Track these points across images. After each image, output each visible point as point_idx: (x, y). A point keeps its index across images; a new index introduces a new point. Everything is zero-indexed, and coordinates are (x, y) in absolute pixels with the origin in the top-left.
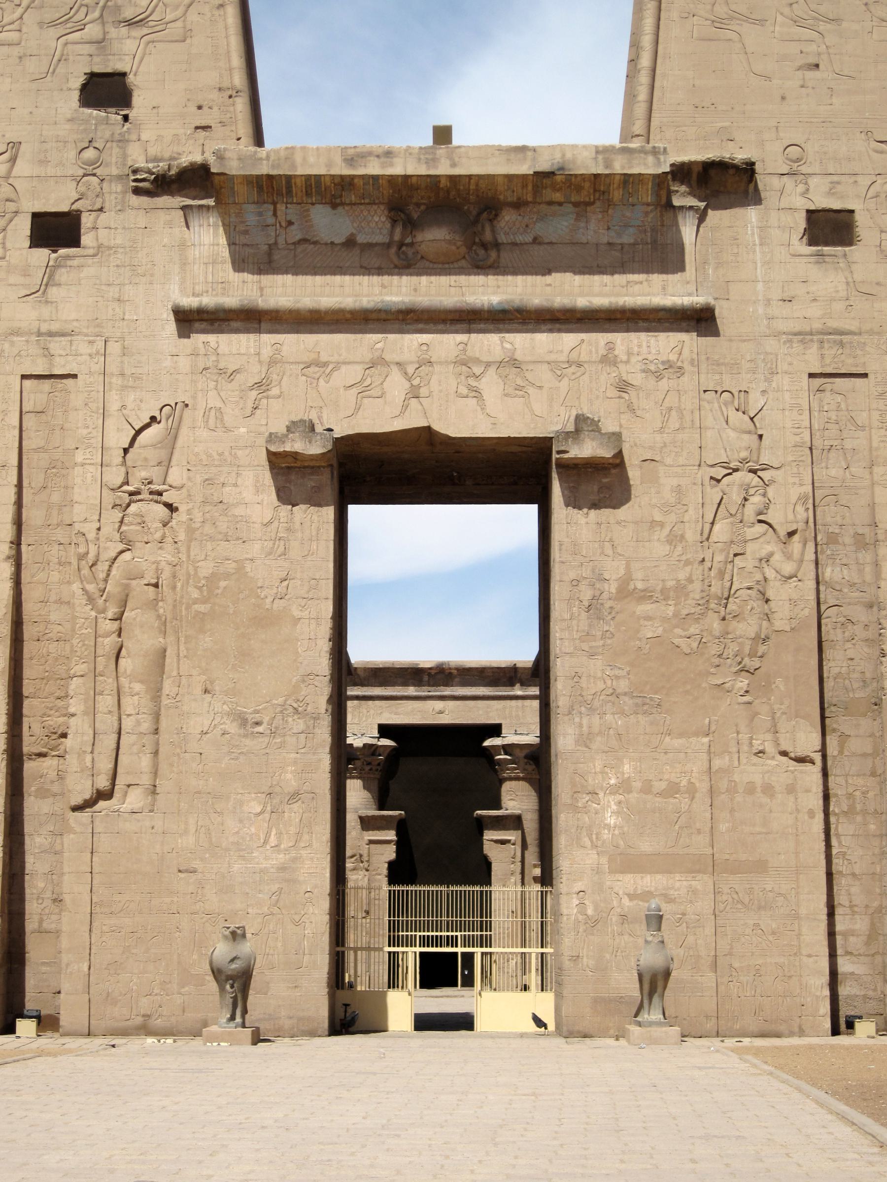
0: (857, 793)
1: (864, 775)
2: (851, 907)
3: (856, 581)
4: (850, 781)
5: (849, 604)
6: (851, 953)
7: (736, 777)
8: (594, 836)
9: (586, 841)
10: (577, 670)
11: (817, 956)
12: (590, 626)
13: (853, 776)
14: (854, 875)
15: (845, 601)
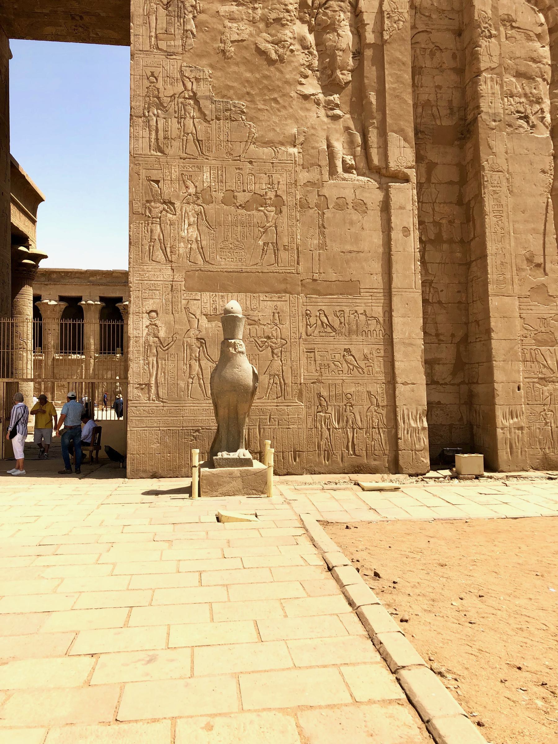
0: (444, 221)
1: (451, 203)
2: (437, 335)
3: (444, 8)
4: (437, 209)
5: (438, 30)
6: (437, 383)
7: (325, 191)
8: (168, 250)
9: (159, 255)
10: (153, 69)
11: (413, 384)
12: (168, 23)
13: (440, 203)
14: (440, 302)
15: (433, 27)
